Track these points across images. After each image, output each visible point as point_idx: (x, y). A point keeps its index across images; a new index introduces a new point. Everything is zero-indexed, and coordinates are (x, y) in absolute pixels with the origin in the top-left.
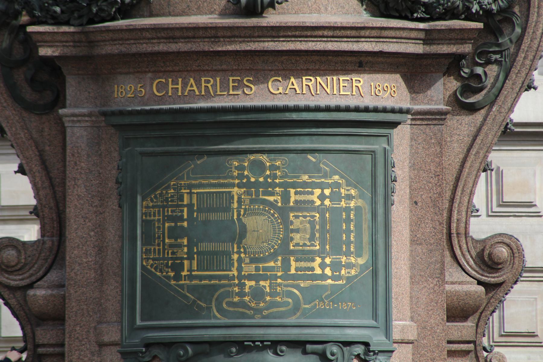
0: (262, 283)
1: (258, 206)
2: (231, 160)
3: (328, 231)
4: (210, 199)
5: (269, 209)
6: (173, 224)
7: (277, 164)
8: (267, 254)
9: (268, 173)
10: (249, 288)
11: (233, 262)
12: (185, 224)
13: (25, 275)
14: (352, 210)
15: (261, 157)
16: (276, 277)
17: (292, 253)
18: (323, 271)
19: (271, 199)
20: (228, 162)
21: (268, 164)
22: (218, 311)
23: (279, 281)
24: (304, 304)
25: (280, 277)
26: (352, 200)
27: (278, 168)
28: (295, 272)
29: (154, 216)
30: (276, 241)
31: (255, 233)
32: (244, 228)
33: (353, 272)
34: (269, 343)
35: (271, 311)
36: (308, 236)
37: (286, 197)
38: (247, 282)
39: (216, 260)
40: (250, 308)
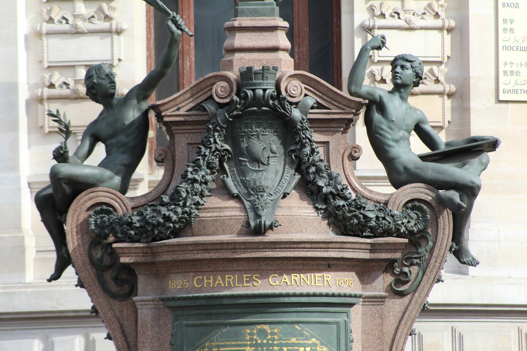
9: (269, 337)
21: (269, 331)
27: (276, 334)
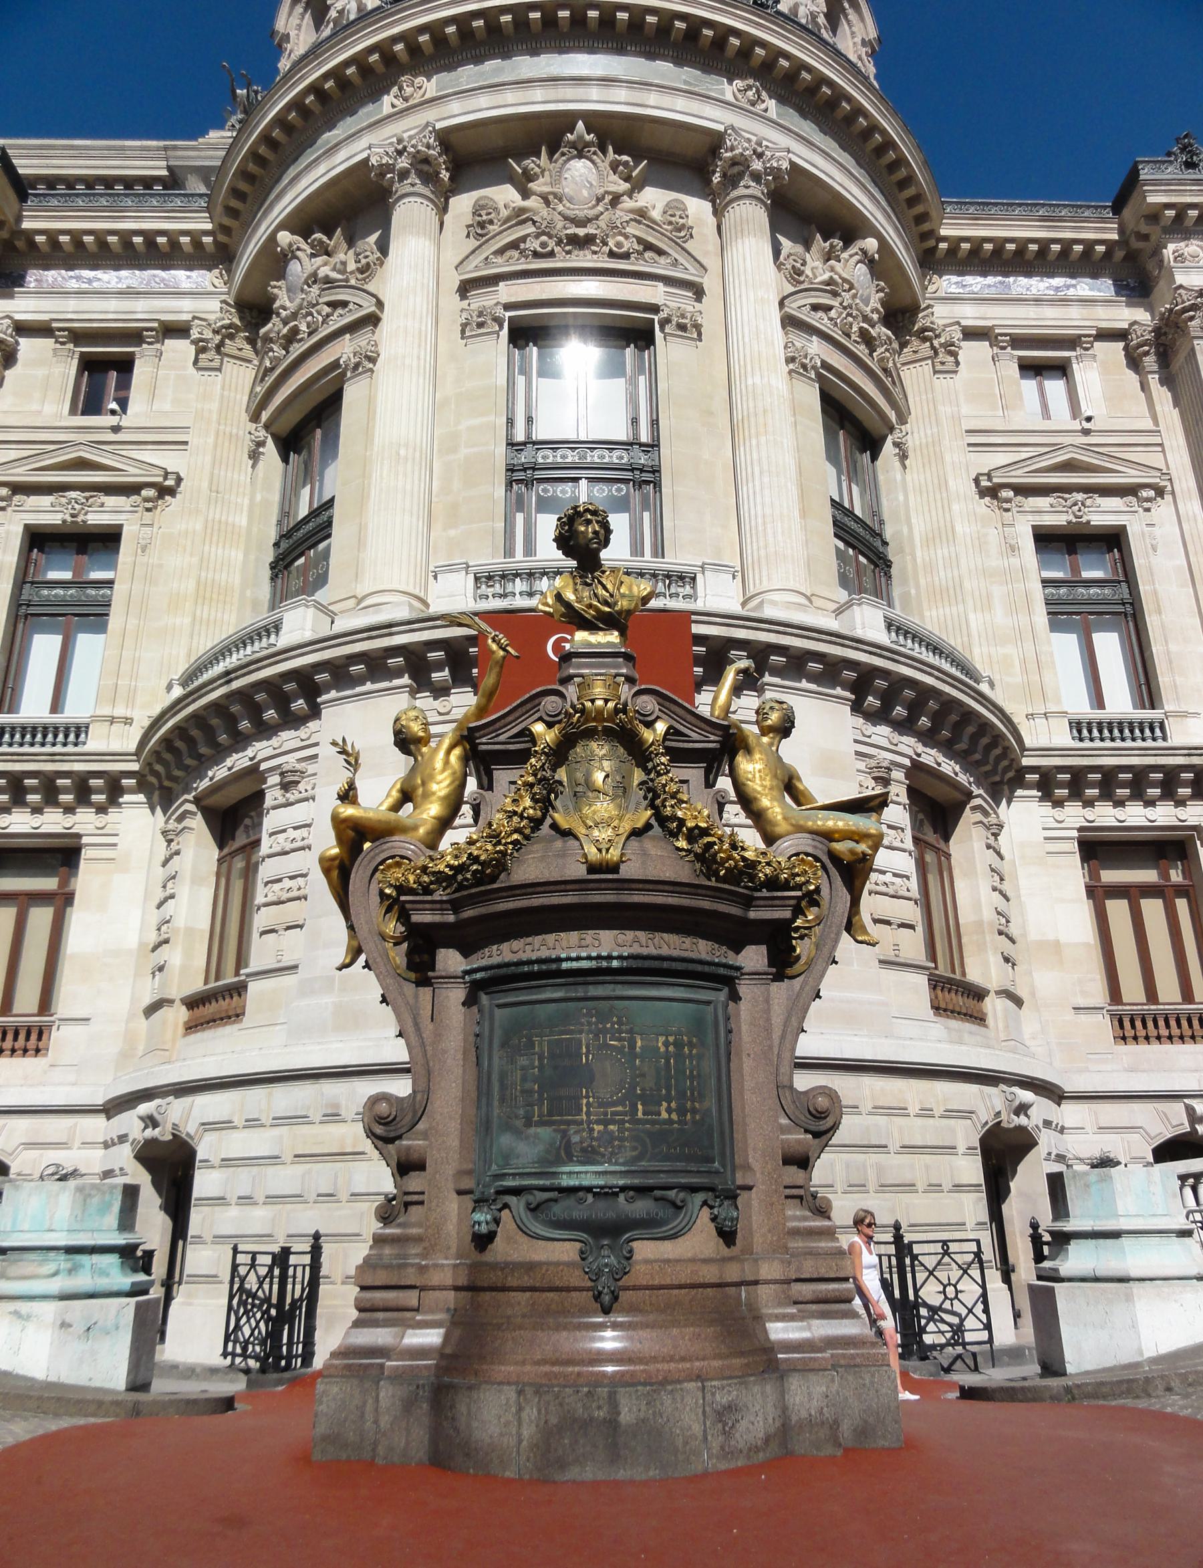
0: (611, 1127)
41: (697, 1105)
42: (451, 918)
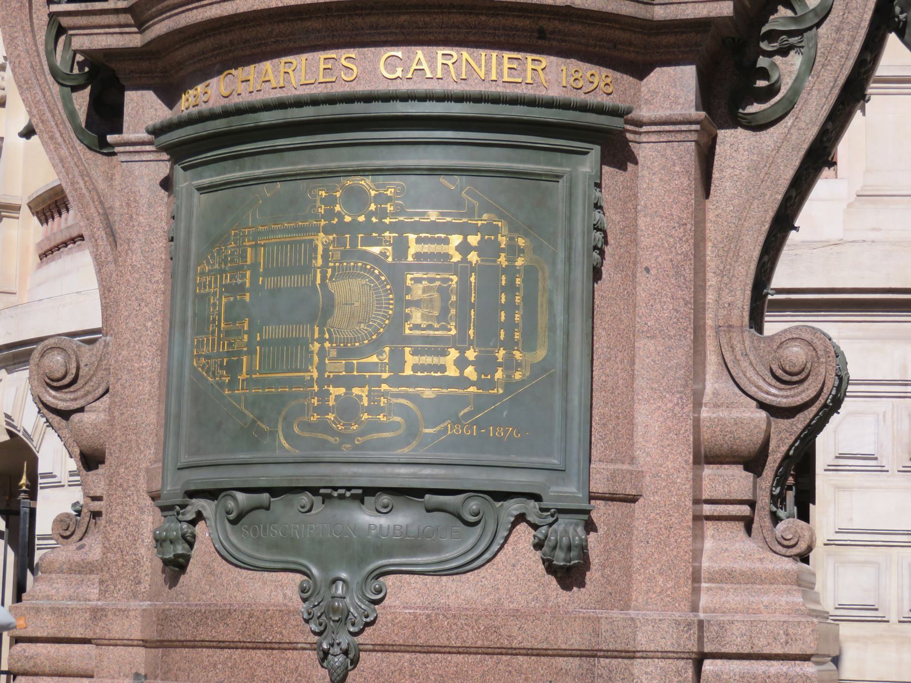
0: (356, 391)
1: (355, 263)
2: (315, 188)
3: (472, 306)
4: (282, 253)
5: (372, 267)
6: (232, 299)
7: (388, 193)
8: (366, 342)
9: (373, 207)
10: (335, 400)
11: (312, 357)
12: (247, 298)
13: (79, 394)
14: (518, 271)
15: (363, 182)
16: (379, 381)
17: (409, 340)
18: (462, 372)
19: (376, 250)
20: (310, 192)
21: (373, 193)
22: (286, 439)
23: (384, 387)
24: (426, 428)
25: (385, 381)
26: (519, 256)
27: (389, 199)
28: (412, 373)
29: (210, 287)
30: (381, 320)
31: (348, 308)
32: (330, 298)
33: (518, 376)
34: (360, 491)
35: (368, 437)
36: (436, 313)
37: (401, 247)
38: (331, 389)
39: (290, 351)
40: (335, 433)
41: (518, 355)
42: (135, 40)
